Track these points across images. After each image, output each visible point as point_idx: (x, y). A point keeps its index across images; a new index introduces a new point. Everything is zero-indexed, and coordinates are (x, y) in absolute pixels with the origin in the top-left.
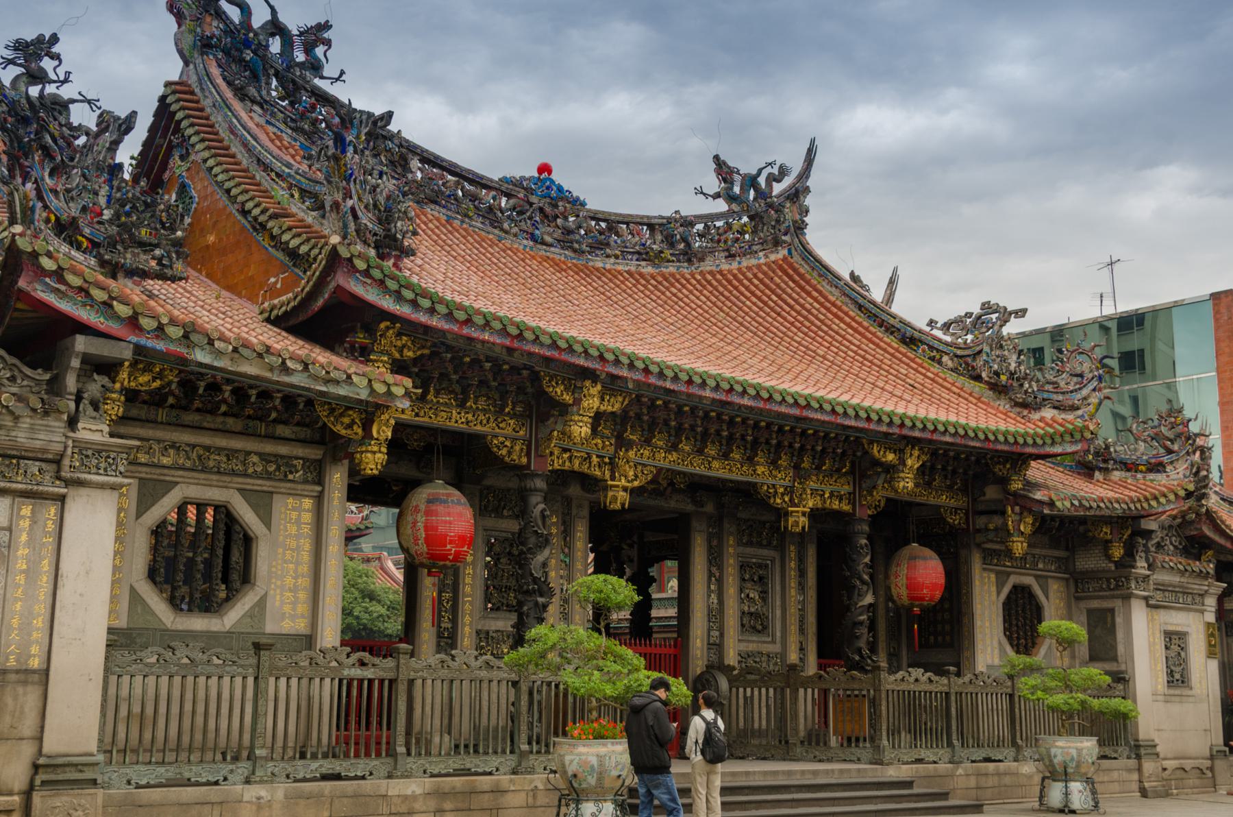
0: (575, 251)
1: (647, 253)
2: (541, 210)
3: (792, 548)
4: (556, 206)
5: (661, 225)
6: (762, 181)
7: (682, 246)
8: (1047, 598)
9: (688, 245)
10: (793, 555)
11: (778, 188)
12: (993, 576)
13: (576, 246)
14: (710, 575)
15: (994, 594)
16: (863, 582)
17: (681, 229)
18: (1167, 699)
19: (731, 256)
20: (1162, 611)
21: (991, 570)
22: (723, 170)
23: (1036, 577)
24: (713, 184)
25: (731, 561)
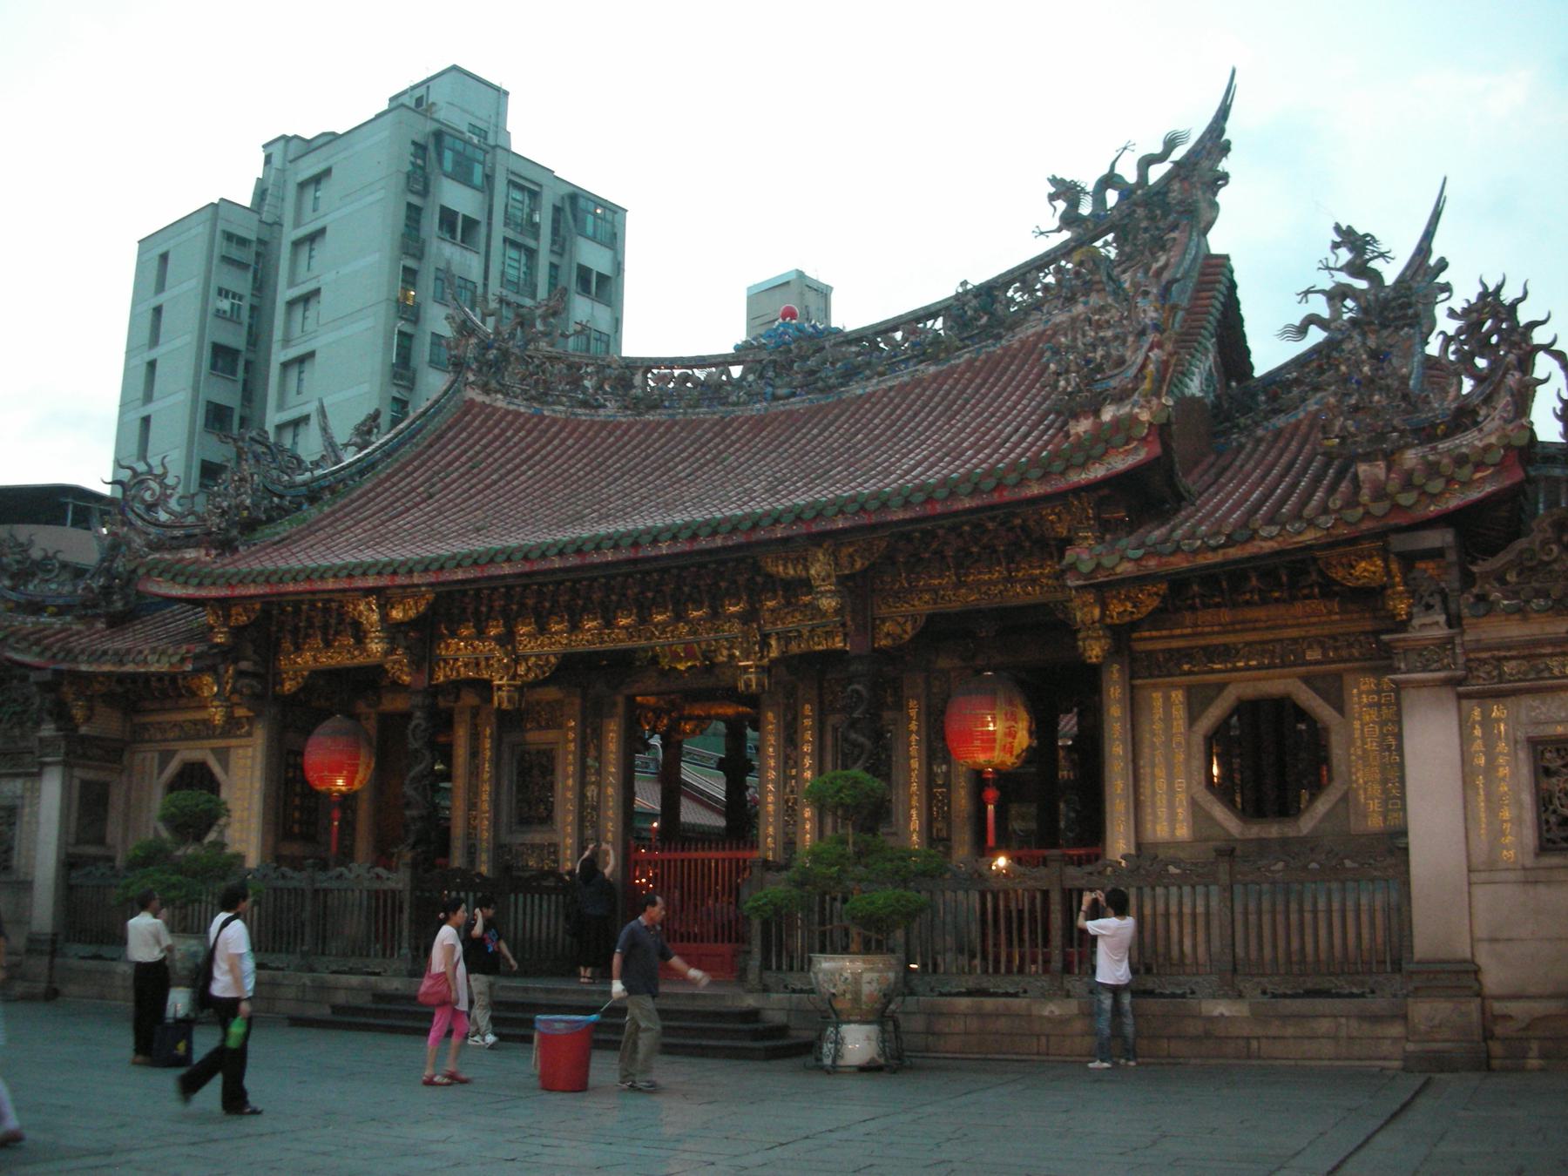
0: (821, 391)
1: (924, 353)
2: (775, 362)
3: (912, 703)
4: (790, 351)
5: (947, 308)
6: (1131, 177)
7: (984, 320)
8: (1340, 708)
9: (992, 314)
10: (913, 713)
11: (1156, 173)
12: (1178, 696)
13: (820, 384)
14: (787, 757)
15: (1179, 724)
16: (855, 744)
17: (974, 303)
18: (1530, 878)
19: (1071, 300)
20: (1528, 701)
21: (1175, 686)
22: (1065, 191)
23: (1307, 680)
24: (1050, 215)
25: (808, 736)
